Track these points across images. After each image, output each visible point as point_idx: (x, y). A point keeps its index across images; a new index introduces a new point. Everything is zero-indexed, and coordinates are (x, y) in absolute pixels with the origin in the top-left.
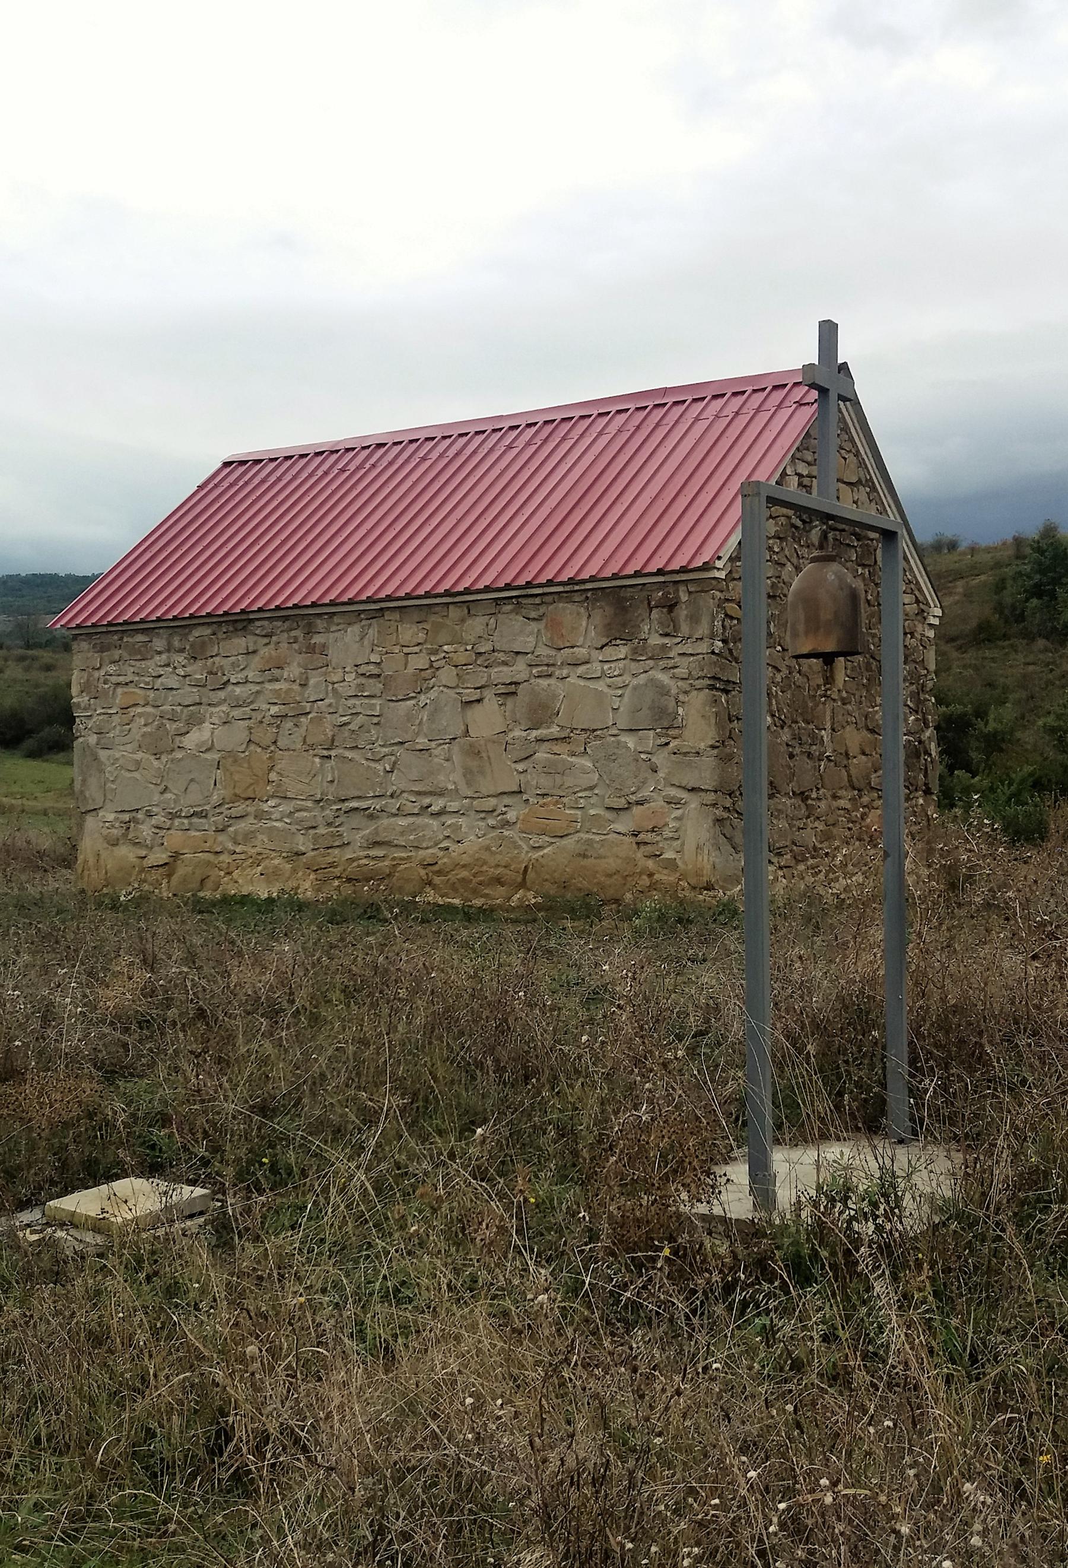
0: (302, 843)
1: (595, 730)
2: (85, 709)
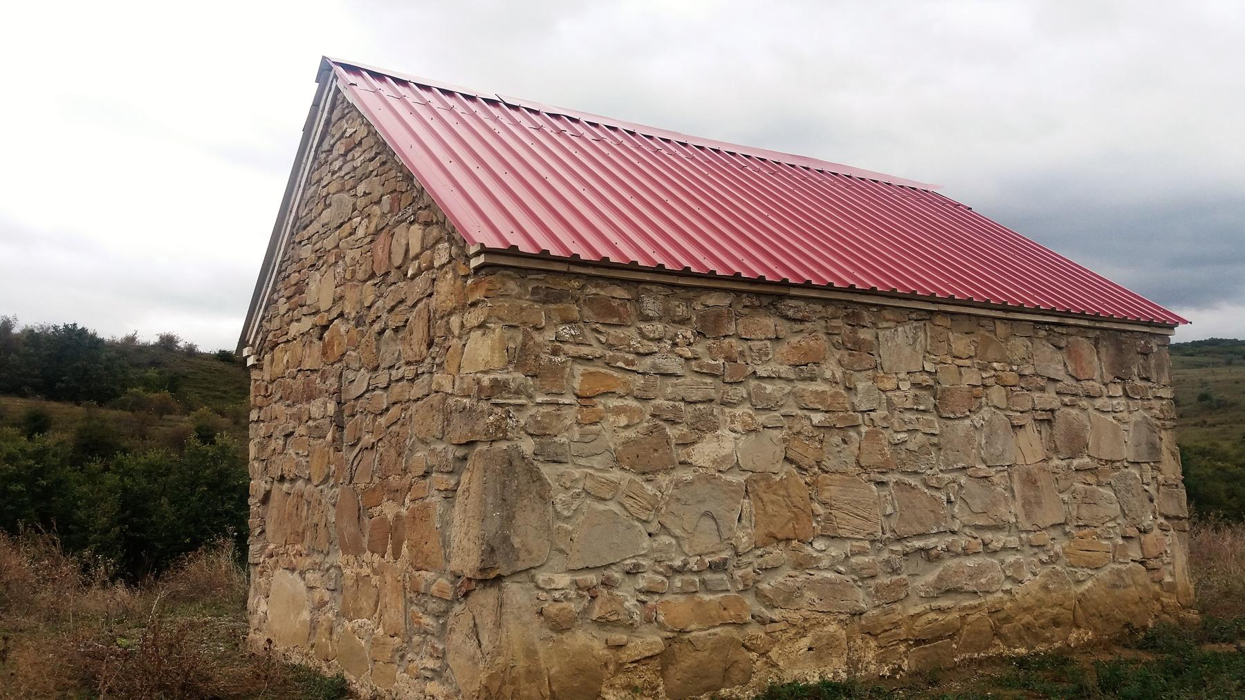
0: (861, 598)
1: (1114, 462)
2: (518, 393)
